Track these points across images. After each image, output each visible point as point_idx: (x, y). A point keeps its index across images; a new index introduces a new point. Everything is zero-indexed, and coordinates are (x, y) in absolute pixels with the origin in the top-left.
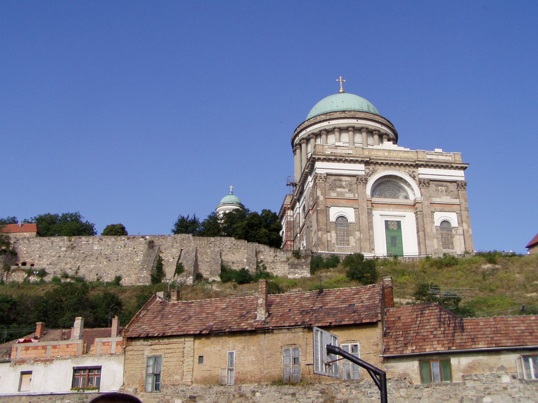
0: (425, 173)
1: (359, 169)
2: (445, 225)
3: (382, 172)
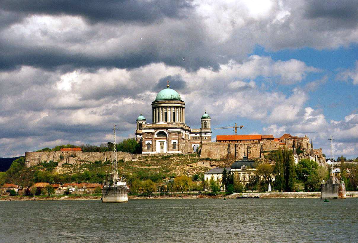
0: (170, 130)
1: (153, 131)
2: (175, 143)
3: (159, 131)
